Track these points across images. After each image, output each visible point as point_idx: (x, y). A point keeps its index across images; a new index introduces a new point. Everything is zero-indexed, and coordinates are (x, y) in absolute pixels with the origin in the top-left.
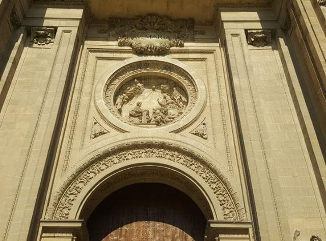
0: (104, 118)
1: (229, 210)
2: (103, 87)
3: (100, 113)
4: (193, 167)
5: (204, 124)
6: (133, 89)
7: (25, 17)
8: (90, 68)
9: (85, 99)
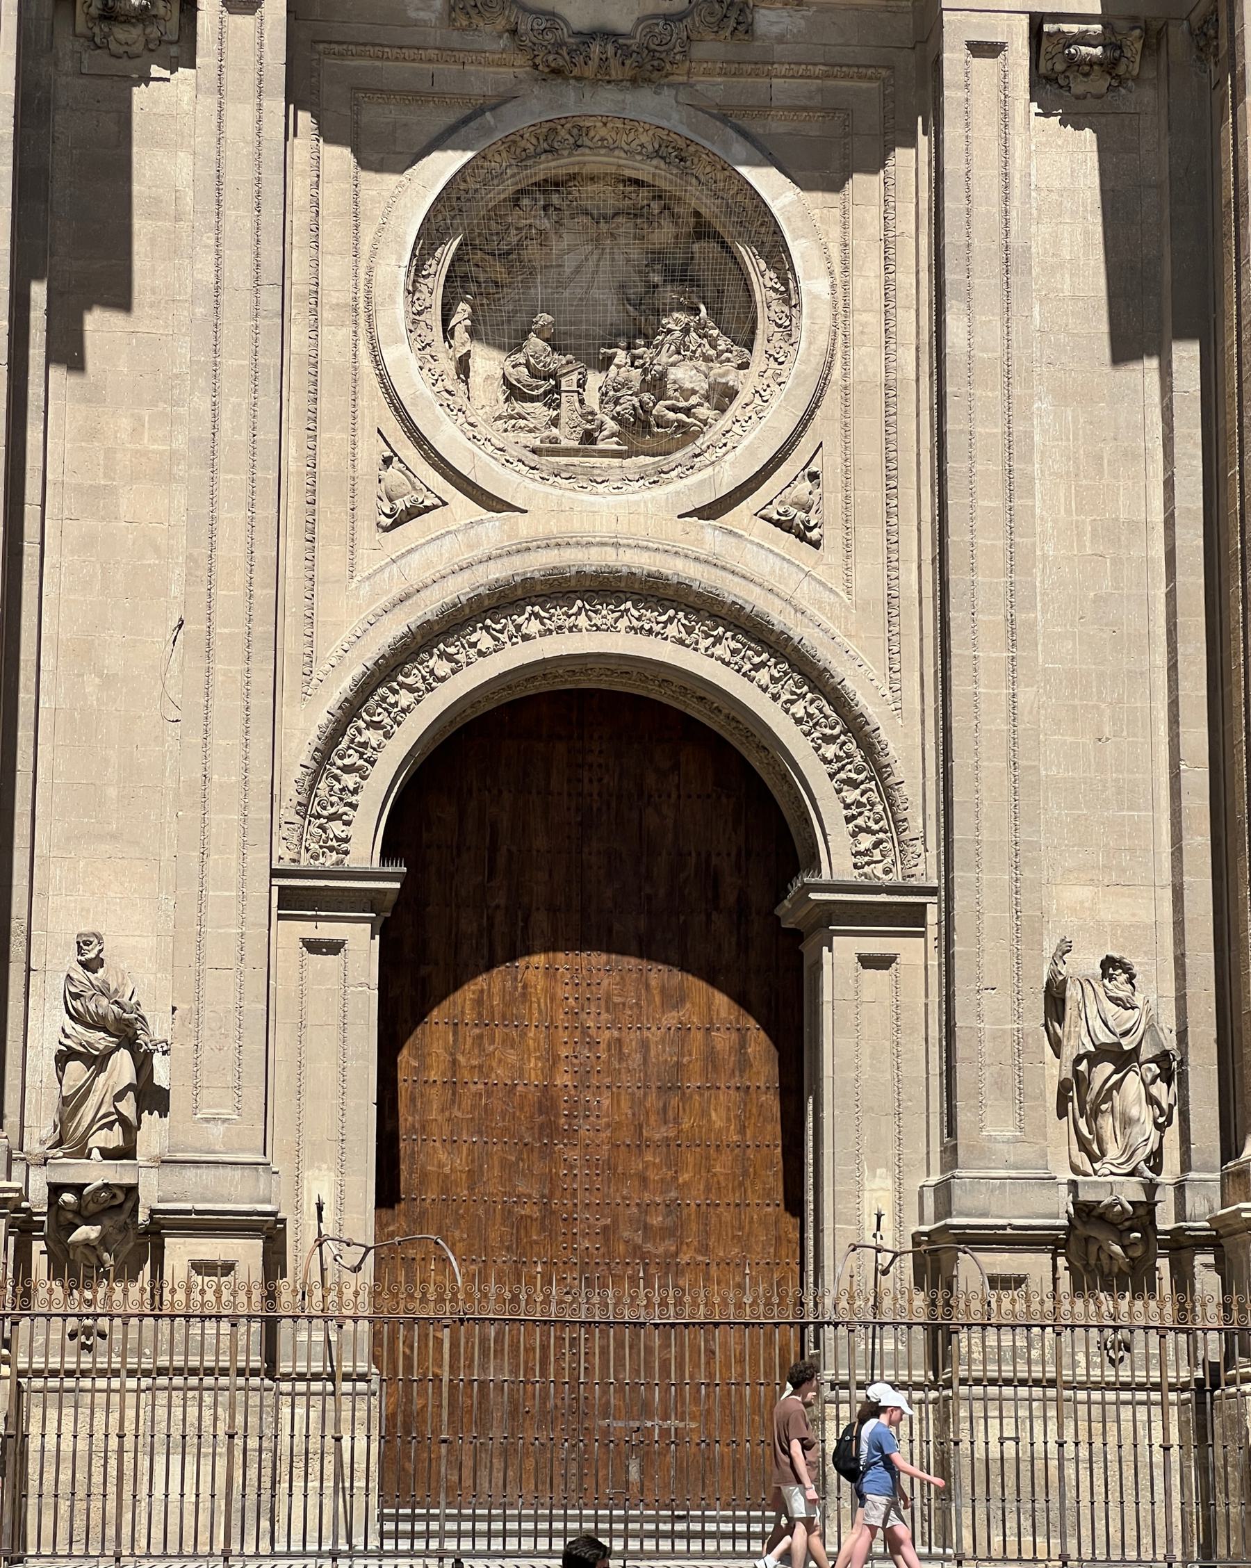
0: (419, 440)
1: (874, 838)
2: (402, 278)
4: (763, 676)
5: (813, 476)
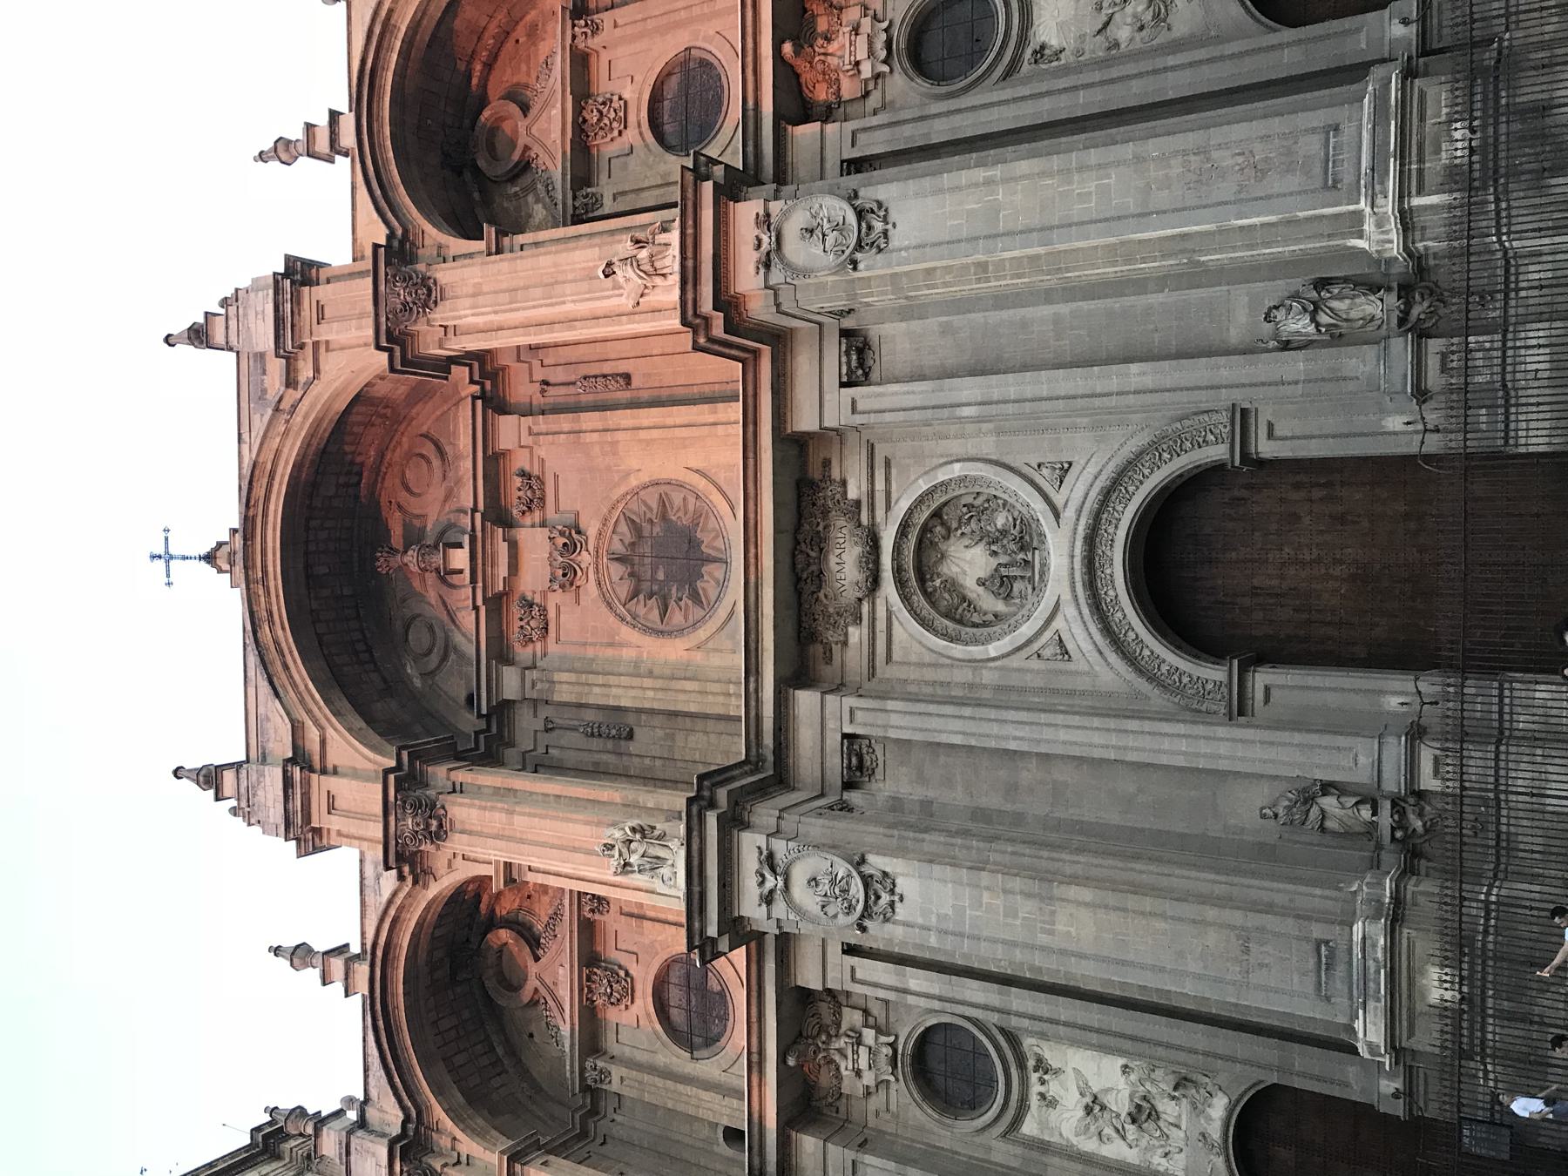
3: (1019, 649)
4: (1131, 489)
6: (946, 596)
7: (822, 795)
8: (913, 674)
9: (988, 676)
